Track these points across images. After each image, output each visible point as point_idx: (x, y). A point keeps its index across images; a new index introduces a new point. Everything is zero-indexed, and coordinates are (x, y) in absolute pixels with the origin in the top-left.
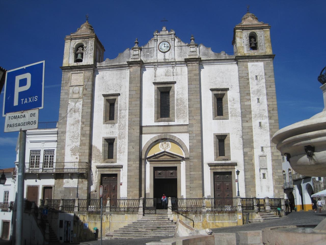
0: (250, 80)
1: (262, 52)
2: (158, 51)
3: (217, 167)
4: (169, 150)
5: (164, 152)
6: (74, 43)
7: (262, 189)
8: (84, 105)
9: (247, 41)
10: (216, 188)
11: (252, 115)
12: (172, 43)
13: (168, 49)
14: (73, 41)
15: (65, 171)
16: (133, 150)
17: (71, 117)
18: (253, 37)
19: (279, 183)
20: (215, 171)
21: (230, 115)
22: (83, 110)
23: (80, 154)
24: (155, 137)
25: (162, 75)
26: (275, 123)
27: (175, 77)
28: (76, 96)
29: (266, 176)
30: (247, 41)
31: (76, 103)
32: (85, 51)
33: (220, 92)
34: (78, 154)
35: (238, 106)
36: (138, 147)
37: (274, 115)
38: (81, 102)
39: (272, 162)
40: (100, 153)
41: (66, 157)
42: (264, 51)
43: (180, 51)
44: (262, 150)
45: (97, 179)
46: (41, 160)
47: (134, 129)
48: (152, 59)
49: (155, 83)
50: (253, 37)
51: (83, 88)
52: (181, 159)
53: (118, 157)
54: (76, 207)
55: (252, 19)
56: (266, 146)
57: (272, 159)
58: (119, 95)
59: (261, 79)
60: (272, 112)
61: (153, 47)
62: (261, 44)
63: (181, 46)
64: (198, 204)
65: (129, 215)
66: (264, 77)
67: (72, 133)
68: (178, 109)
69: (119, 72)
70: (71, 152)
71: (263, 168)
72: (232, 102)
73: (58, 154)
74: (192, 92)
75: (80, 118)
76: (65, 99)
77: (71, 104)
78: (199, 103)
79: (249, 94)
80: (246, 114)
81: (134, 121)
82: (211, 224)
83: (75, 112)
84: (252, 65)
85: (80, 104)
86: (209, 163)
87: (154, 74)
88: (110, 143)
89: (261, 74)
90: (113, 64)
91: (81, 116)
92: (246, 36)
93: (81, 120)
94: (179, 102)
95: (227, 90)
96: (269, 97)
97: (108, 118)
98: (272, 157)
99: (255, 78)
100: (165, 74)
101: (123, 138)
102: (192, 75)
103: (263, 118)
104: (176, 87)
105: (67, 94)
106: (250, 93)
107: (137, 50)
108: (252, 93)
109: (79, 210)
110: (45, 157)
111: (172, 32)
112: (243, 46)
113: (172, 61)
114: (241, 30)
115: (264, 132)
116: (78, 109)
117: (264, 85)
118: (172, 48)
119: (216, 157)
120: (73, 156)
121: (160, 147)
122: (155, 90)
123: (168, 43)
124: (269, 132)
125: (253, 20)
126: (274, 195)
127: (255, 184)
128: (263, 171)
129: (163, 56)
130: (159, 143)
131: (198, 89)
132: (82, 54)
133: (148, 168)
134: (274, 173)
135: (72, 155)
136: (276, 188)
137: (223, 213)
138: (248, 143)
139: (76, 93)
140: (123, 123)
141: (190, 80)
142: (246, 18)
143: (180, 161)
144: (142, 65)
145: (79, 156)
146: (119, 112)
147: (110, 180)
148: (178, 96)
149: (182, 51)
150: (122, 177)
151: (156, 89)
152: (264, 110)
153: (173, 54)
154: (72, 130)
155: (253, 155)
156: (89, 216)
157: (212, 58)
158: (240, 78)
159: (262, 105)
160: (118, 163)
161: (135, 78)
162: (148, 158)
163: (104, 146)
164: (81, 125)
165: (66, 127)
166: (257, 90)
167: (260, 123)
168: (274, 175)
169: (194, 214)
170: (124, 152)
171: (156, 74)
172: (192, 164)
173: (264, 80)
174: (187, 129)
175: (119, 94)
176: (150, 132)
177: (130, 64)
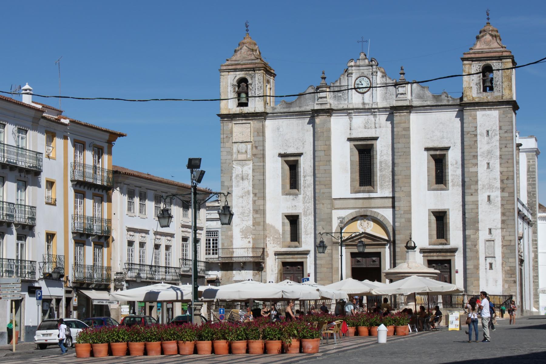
0: (479, 136)
3: (432, 254)
4: (371, 230)
5: (363, 233)
15: (235, 260)
17: (238, 186)
18: (487, 70)
19: (510, 276)
20: (430, 258)
22: (253, 176)
23: (254, 237)
24: (351, 213)
25: (359, 127)
27: (377, 129)
28: (241, 157)
29: (493, 266)
31: (243, 166)
33: (438, 153)
34: (251, 237)
37: (508, 185)
38: (251, 166)
39: (502, 248)
40: (279, 234)
41: (234, 242)
43: (385, 91)
44: (490, 232)
45: (277, 269)
47: (323, 204)
49: (350, 140)
50: (487, 70)
51: (252, 145)
55: (490, 38)
58: (300, 155)
59: (494, 136)
60: (505, 181)
62: (498, 83)
68: (382, 176)
69: (300, 121)
70: (241, 234)
71: (490, 256)
72: (455, 166)
73: (224, 237)
75: (251, 188)
76: (228, 161)
77: (237, 170)
81: (324, 193)
83: (243, 179)
84: (483, 115)
87: (349, 126)
88: (293, 220)
90: (292, 110)
91: (251, 185)
95: (447, 149)
96: (503, 161)
97: (288, 186)
98: (502, 242)
99: (485, 134)
101: (309, 215)
105: (230, 153)
106: (477, 156)
111: (373, 63)
113: (373, 107)
114: (470, 62)
116: (247, 176)
117: (498, 144)
122: (351, 149)
125: (493, 39)
127: (479, 277)
128: (489, 260)
130: (357, 220)
135: (242, 238)
139: (242, 153)
142: (483, 36)
143: (385, 245)
145: (253, 239)
149: (388, 92)
157: (429, 103)
160: (304, 247)
161: (323, 132)
163: (283, 224)
167: (489, 197)
168: (504, 266)
173: (498, 137)
175: (302, 154)
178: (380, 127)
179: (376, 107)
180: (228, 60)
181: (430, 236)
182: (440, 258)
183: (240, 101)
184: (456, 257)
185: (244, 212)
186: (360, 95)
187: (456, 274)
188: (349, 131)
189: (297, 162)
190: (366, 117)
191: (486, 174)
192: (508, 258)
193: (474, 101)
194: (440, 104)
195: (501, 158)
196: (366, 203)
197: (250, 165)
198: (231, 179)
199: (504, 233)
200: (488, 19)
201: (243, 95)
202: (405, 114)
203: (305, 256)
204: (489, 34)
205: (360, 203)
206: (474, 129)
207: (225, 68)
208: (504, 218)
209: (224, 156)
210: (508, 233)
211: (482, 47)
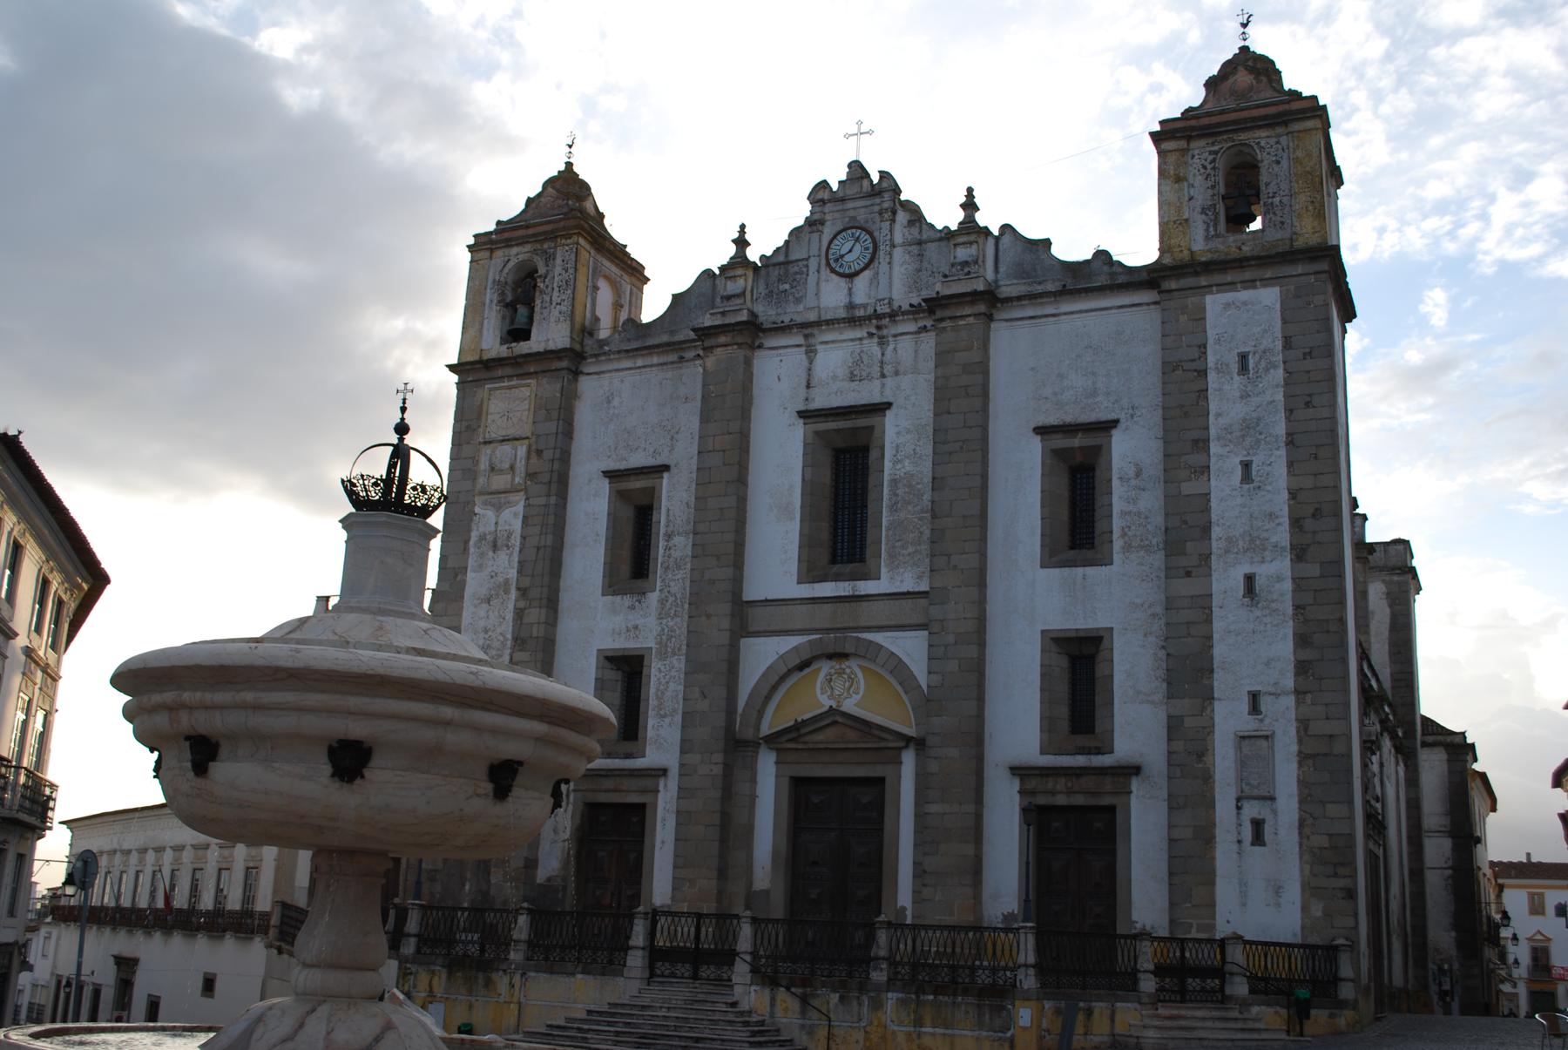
2: (825, 272)
11: (1214, 544)
14: (499, 253)
17: (480, 567)
20: (1042, 800)
21: (1117, 544)
22: (523, 537)
24: (796, 649)
25: (835, 378)
26: (1322, 576)
27: (889, 381)
28: (500, 482)
31: (499, 508)
32: (542, 292)
33: (1077, 441)
35: (1151, 502)
38: (520, 508)
39: (1300, 764)
42: (1287, 235)
44: (1255, 708)
47: (708, 616)
49: (804, 415)
51: (529, 447)
52: (902, 744)
53: (650, 733)
54: (409, 935)
56: (1272, 690)
57: (1300, 752)
59: (1267, 370)
60: (1309, 524)
62: (1277, 200)
63: (920, 243)
64: (958, 950)
65: (589, 979)
67: (482, 635)
69: (669, 375)
71: (1256, 792)
72: (1133, 482)
75: (513, 574)
79: (1202, 444)
80: (1185, 537)
81: (713, 582)
82: (901, 1038)
83: (495, 547)
84: (1227, 306)
85: (515, 515)
86: (1016, 763)
88: (626, 671)
89: (1265, 344)
92: (1204, 167)
95: (1110, 425)
97: (625, 569)
98: (1300, 742)
99: (1235, 367)
101: (674, 654)
108: (1218, 439)
109: (418, 951)
112: (1186, 216)
114: (1182, 144)
115: (1268, 620)
117: (1280, 397)
118: (881, 253)
121: (818, 691)
122: (806, 445)
123: (870, 234)
125: (1259, 81)
126: (1303, 928)
127: (1213, 873)
128: (1251, 810)
133: (767, 782)
134: (1310, 821)
137: (955, 994)
138: (1189, 673)
139: (501, 471)
140: (675, 588)
141: (942, 395)
146: (662, 544)
147: (613, 829)
149: (925, 264)
152: (1271, 516)
154: (482, 623)
155: (1209, 729)
156: (450, 974)
160: (652, 757)
162: (771, 740)
166: (1244, 420)
167: (1250, 579)
168: (1307, 831)
169: (834, 991)
173: (1279, 374)
174: (917, 610)
175: (666, 468)
178: (897, 373)
181: (1048, 723)
182: (1079, 800)
184: (1133, 798)
188: (802, 392)
191: (1239, 500)
195: (1290, 443)
198: (466, 550)
201: (522, 310)
202: (971, 320)
203: (648, 783)
208: (1308, 654)
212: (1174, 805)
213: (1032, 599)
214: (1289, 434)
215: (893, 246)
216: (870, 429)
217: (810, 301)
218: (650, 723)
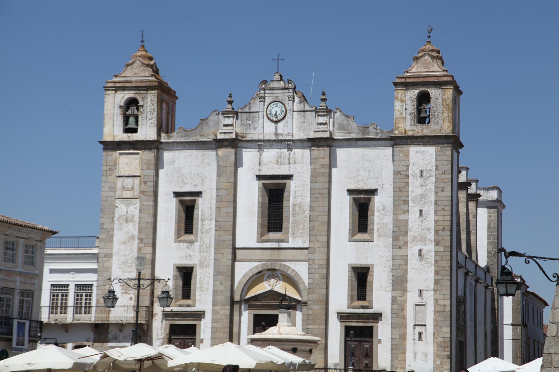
0: (411, 177)
1: (436, 127)
2: (266, 118)
4: (279, 288)
6: (122, 97)
7: (415, 357)
8: (142, 211)
9: (413, 107)
10: (349, 353)
11: (409, 238)
12: (289, 104)
13: (283, 116)
16: (221, 288)
17: (120, 229)
18: (424, 99)
19: (443, 349)
21: (376, 234)
22: (140, 218)
24: (256, 267)
27: (292, 166)
30: (413, 107)
31: (128, 205)
32: (142, 113)
34: (133, 292)
35: (389, 220)
36: (230, 284)
37: (444, 238)
38: (138, 205)
39: (435, 314)
42: (438, 127)
43: (303, 120)
46: (71, 301)
47: (223, 254)
48: (256, 132)
49: (259, 177)
50: (424, 99)
51: (140, 180)
57: (435, 310)
59: (429, 177)
60: (441, 233)
61: (257, 110)
62: (436, 113)
63: (304, 111)
66: (434, 173)
70: (121, 288)
71: (420, 323)
72: (382, 212)
74: (316, 196)
75: (136, 233)
76: (109, 199)
77: (121, 209)
78: (327, 214)
79: (406, 202)
80: (400, 234)
81: (224, 241)
83: (127, 221)
84: (417, 152)
85: (136, 208)
86: (339, 312)
87: (258, 160)
88: (186, 274)
89: (429, 167)
90: (191, 140)
91: (137, 229)
93: (138, 235)
94: (296, 209)
95: (373, 192)
96: (439, 208)
98: (435, 307)
99: (419, 175)
100: (275, 160)
101: (206, 267)
102: (317, 166)
103: (426, 242)
104: (292, 185)
105: (113, 189)
107: (231, 117)
110: (78, 297)
112: (404, 116)
113: (288, 138)
115: (426, 265)
116: (133, 217)
117: (433, 187)
118: (289, 114)
119: (350, 301)
120: (124, 294)
122: (259, 188)
124: (433, 267)
125: (433, 61)
128: (418, 329)
129: (274, 127)
131: (327, 191)
132: (137, 118)
134: (437, 333)
135: (122, 293)
136: (437, 357)
138: (399, 282)
139: (128, 190)
140: (206, 241)
141: (314, 175)
142: (421, 57)
144: (236, 143)
146: (200, 223)
148: (296, 199)
149: (306, 120)
150: (204, 330)
151: (261, 186)
152: (429, 229)
153: (290, 126)
155: (405, 302)
157: (354, 136)
158: (396, 173)
159: (425, 221)
160: (198, 307)
163: (175, 278)
164: (138, 244)
165: (112, 246)
166: (421, 194)
167: (420, 251)
168: (436, 336)
170: (207, 289)
171: (262, 159)
172: (310, 312)
173: (433, 179)
175: (201, 193)
176: (249, 259)
177: (219, 144)
178: (295, 163)
179: (291, 138)
180: (116, 76)
183: (128, 127)
185: (127, 262)
186: (273, 124)
187: (379, 345)
188: (258, 167)
189: (195, 200)
190: (279, 151)
191: (418, 223)
192: (441, 327)
193: (407, 135)
194: (366, 137)
195: (436, 204)
196: (275, 255)
197: (137, 203)
198: (113, 221)
199: (438, 296)
200: (429, 37)
201: (132, 120)
204: (429, 54)
205: (267, 255)
206: (405, 168)
207: (110, 85)
208: (438, 277)
209: (105, 192)
210: (442, 296)
211: (419, 70)
212: (394, 327)
213: (345, 253)
214: (436, 201)
215: (293, 111)
216: (285, 184)
217: (260, 130)
218: (197, 293)
